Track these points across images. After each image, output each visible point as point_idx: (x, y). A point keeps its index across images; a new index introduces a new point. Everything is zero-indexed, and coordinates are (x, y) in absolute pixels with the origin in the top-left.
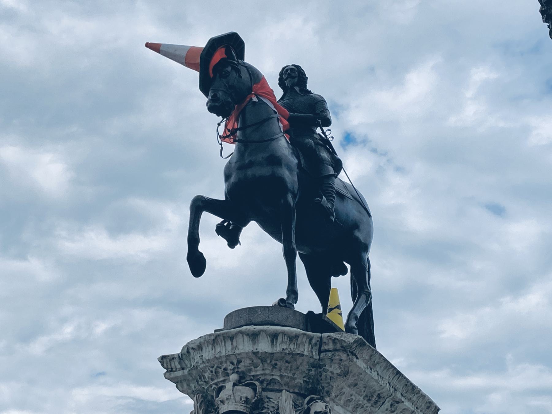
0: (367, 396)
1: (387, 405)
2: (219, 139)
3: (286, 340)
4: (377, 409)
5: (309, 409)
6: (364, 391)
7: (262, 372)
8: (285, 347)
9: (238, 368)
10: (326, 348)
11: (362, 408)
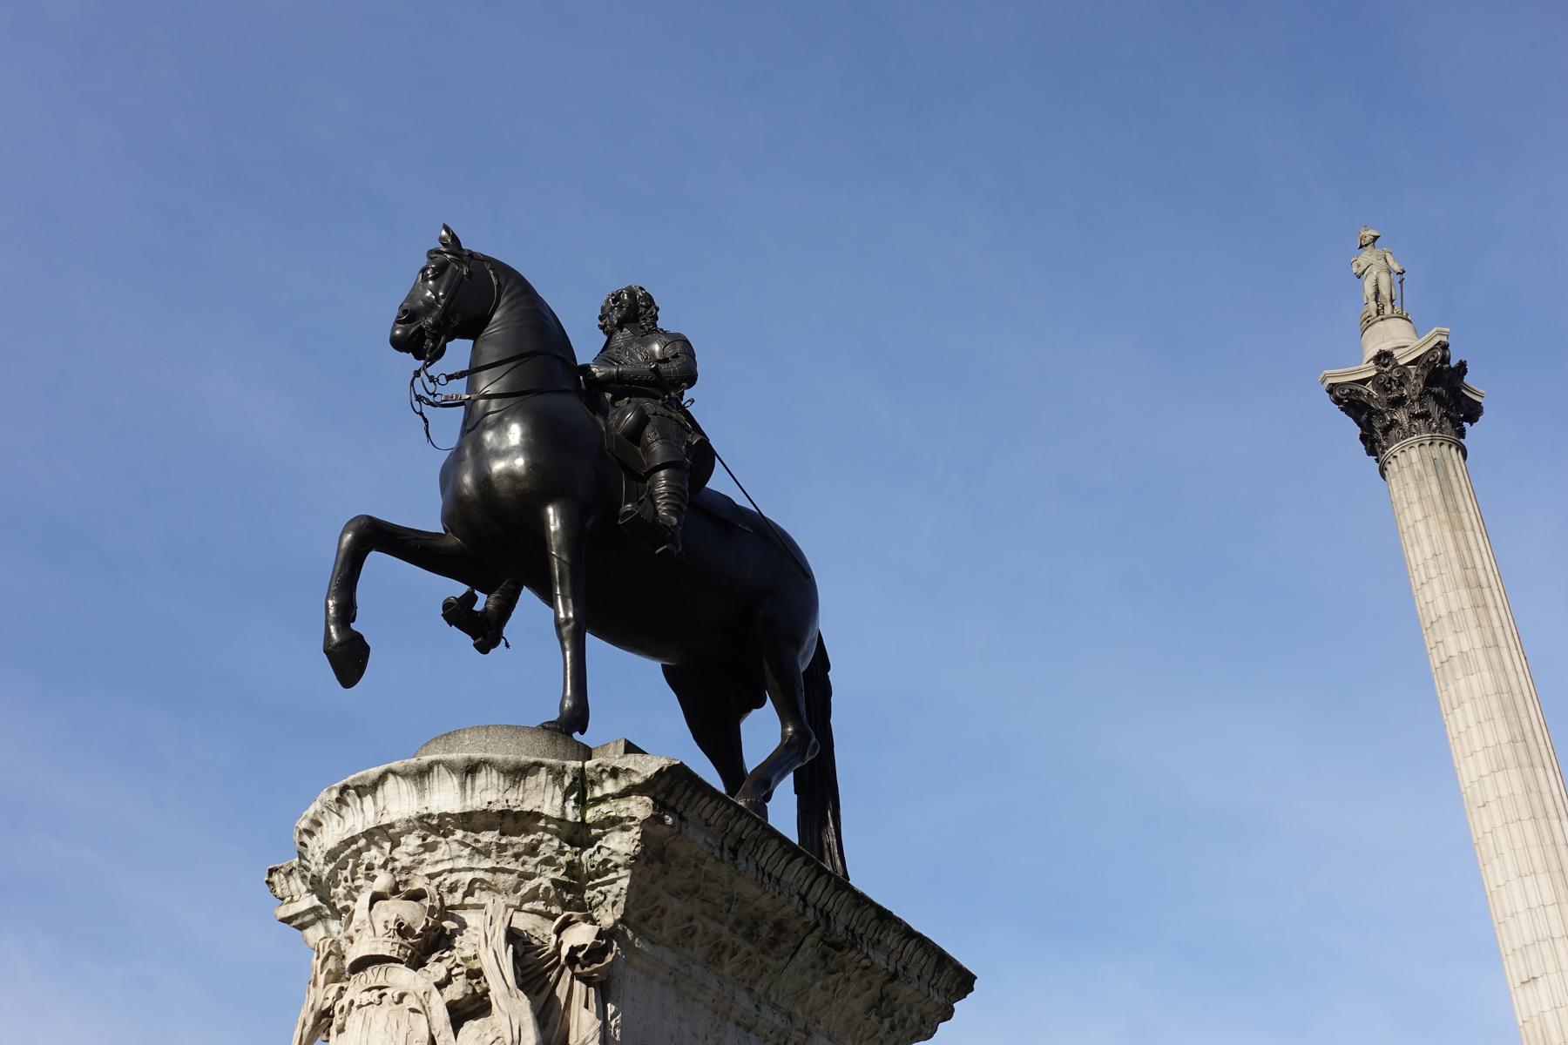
0: (739, 923)
1: (808, 952)
2: (416, 404)
3: (495, 781)
4: (782, 963)
5: (559, 946)
6: (729, 911)
7: (448, 865)
8: (493, 799)
9: (394, 860)
10: (598, 793)
11: (734, 954)
